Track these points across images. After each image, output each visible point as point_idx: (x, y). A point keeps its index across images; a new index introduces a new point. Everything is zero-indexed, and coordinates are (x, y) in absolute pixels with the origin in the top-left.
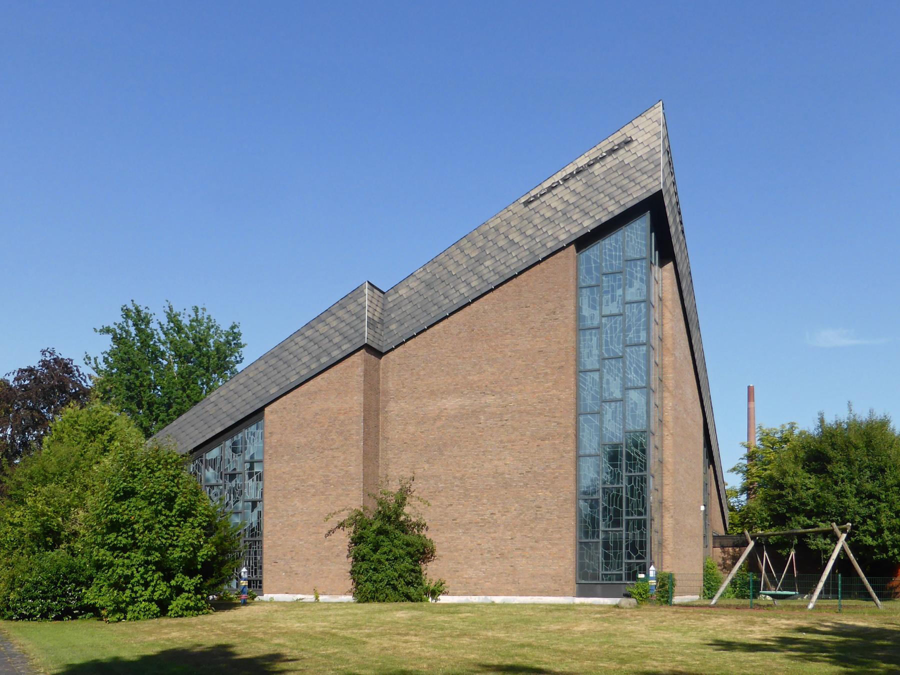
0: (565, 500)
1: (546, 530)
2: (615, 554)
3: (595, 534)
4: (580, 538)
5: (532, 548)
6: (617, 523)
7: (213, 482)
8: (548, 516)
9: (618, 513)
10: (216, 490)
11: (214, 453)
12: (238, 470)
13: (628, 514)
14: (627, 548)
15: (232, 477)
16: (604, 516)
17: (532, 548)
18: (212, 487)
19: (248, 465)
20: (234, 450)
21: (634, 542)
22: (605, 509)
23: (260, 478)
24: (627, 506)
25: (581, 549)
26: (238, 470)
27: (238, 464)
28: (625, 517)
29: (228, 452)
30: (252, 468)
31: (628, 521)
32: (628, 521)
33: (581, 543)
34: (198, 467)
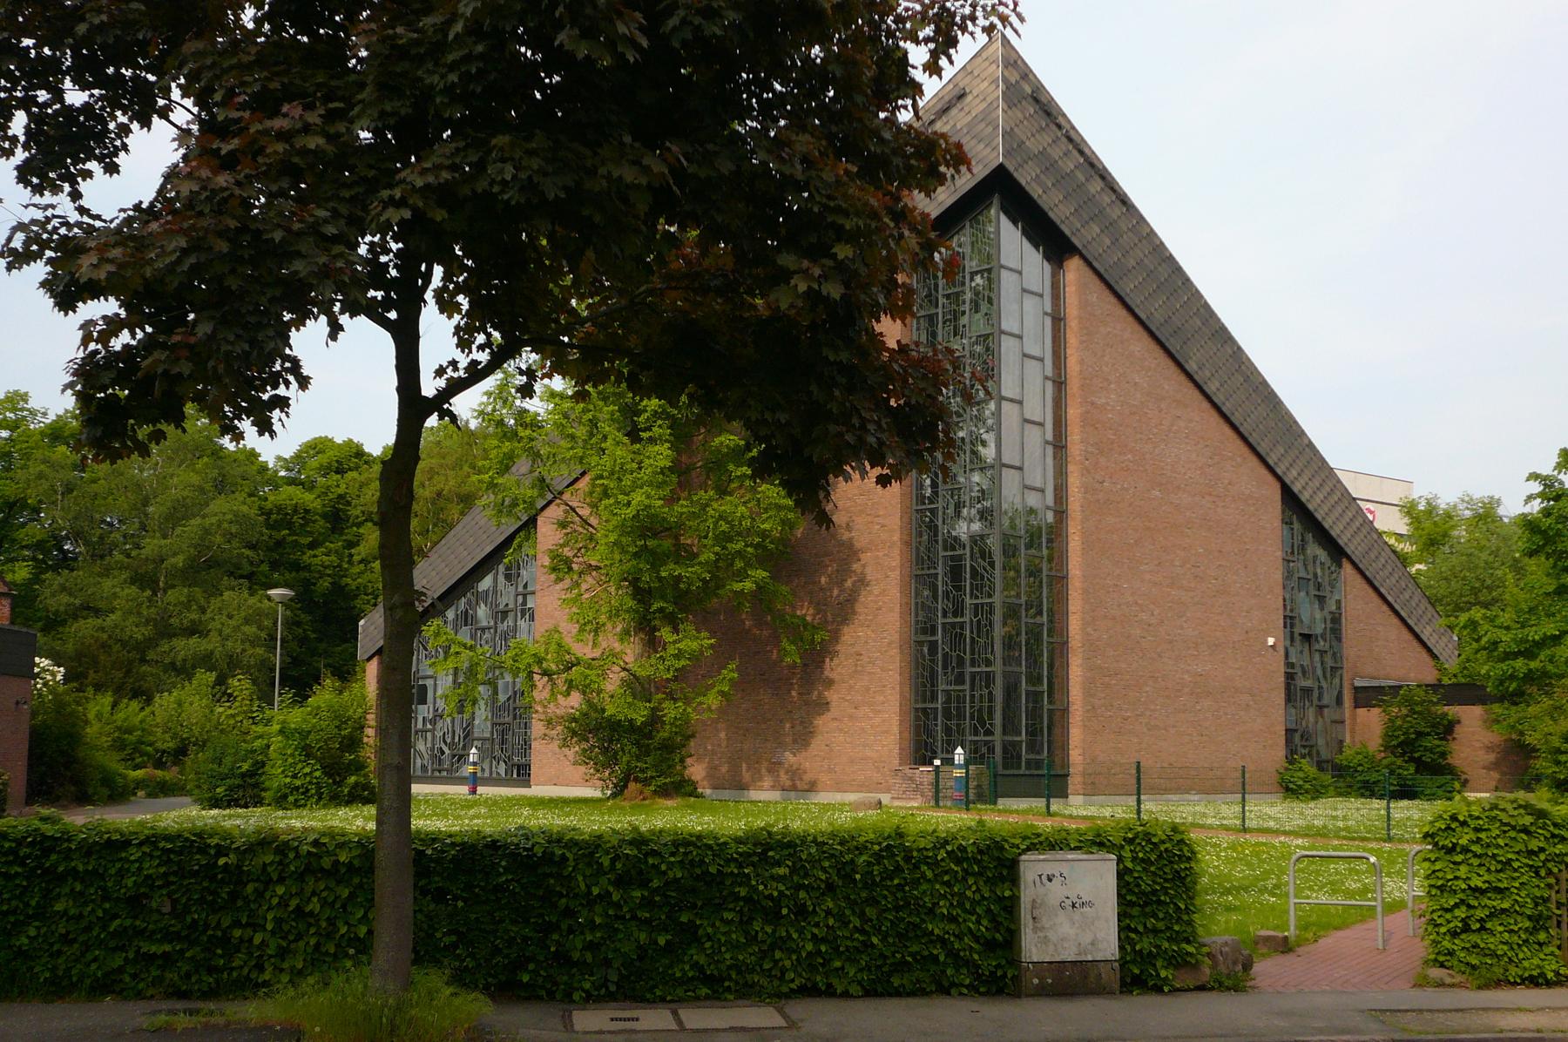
0: (890, 644)
1: (868, 689)
2: (958, 725)
3: (934, 698)
4: (916, 701)
5: (851, 717)
6: (960, 679)
7: (484, 624)
8: (869, 668)
9: (961, 662)
10: (487, 635)
11: (486, 583)
12: (511, 606)
13: (973, 665)
14: (972, 718)
15: (505, 614)
16: (945, 667)
17: (851, 717)
18: (483, 630)
19: (520, 599)
20: (508, 577)
21: (980, 710)
22: (945, 656)
23: (532, 618)
24: (973, 653)
25: (917, 718)
26: (511, 606)
27: (507, 598)
28: (969, 669)
29: (501, 578)
30: (524, 603)
31: (973, 675)
32: (973, 675)
33: (917, 710)
34: (469, 602)
